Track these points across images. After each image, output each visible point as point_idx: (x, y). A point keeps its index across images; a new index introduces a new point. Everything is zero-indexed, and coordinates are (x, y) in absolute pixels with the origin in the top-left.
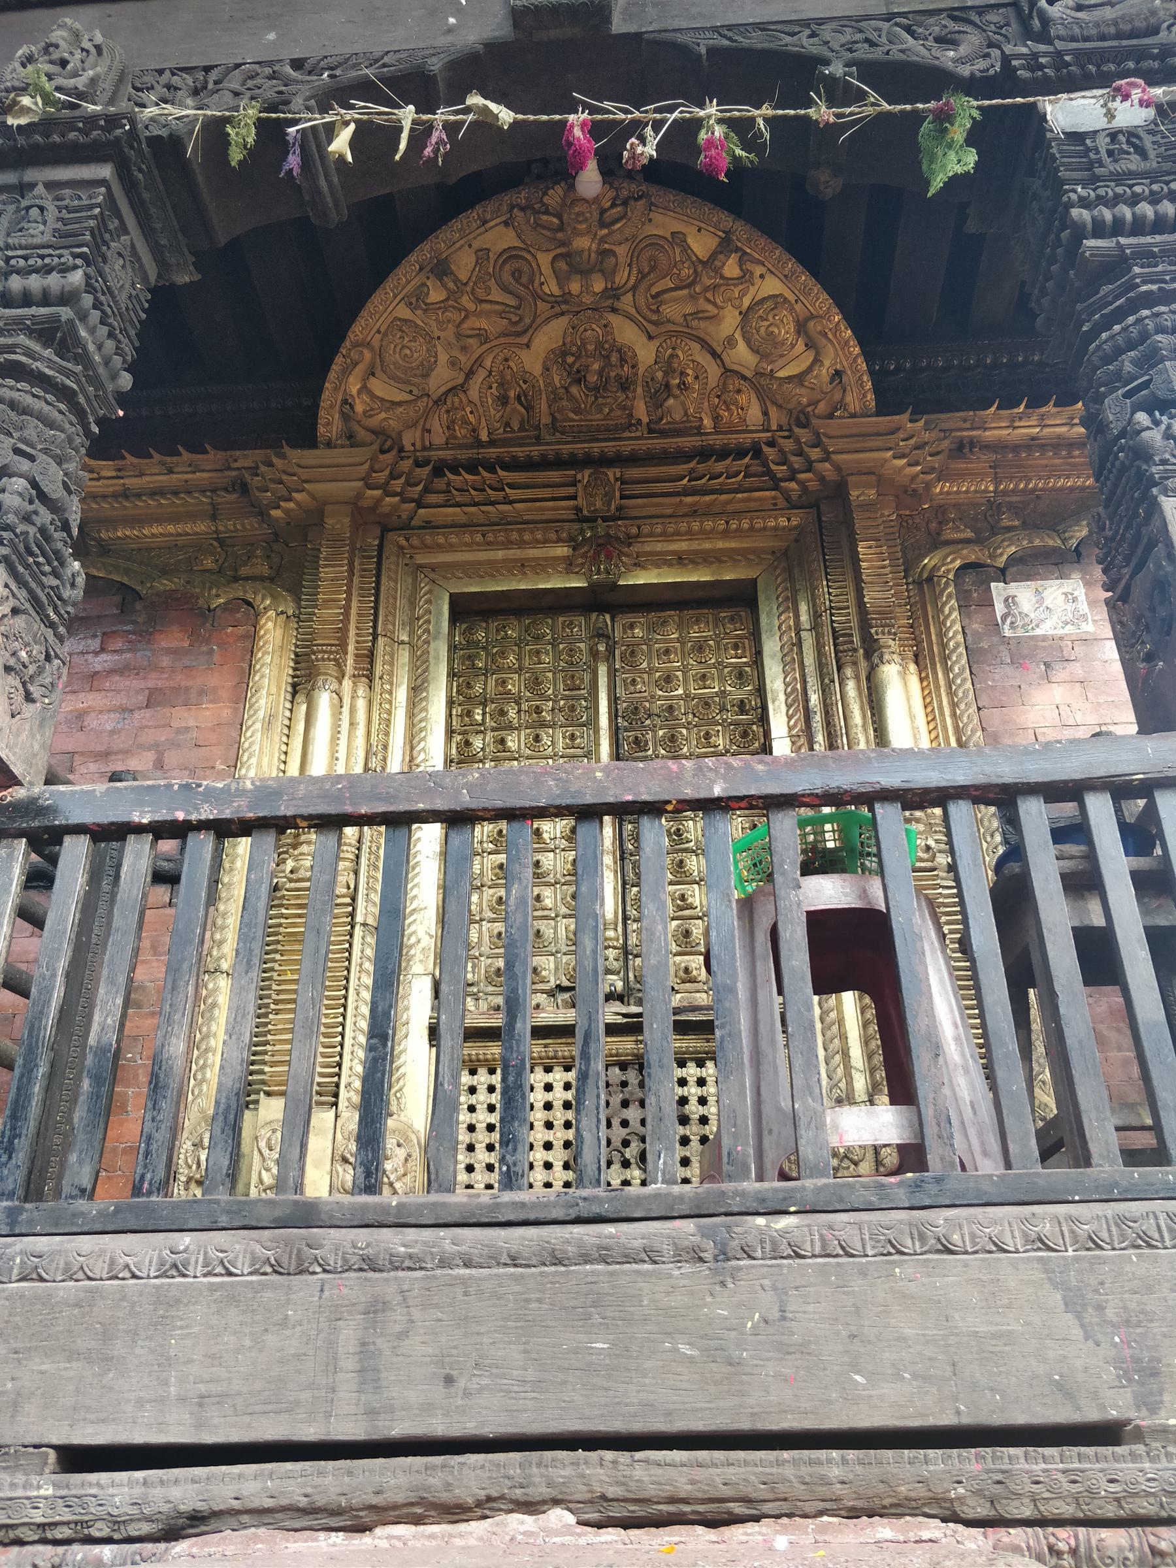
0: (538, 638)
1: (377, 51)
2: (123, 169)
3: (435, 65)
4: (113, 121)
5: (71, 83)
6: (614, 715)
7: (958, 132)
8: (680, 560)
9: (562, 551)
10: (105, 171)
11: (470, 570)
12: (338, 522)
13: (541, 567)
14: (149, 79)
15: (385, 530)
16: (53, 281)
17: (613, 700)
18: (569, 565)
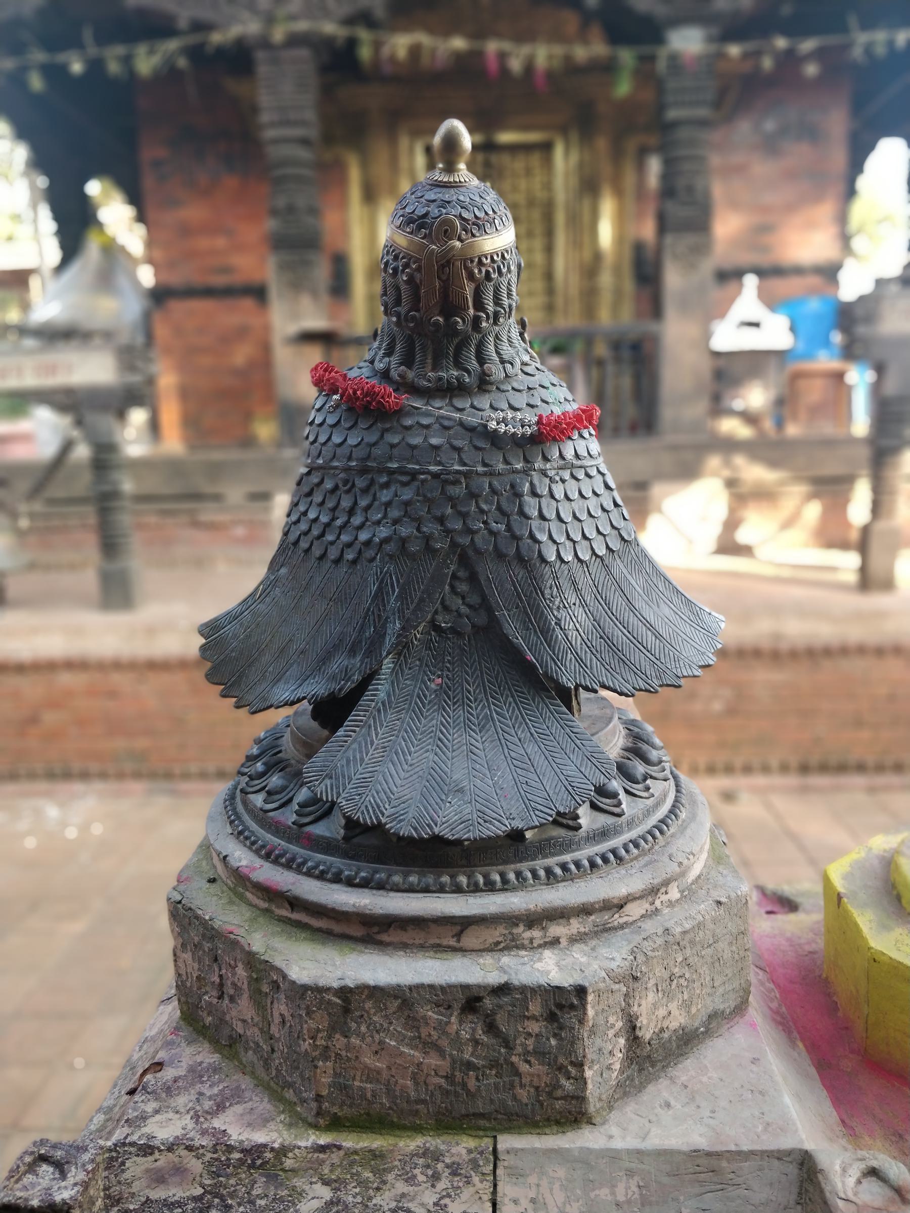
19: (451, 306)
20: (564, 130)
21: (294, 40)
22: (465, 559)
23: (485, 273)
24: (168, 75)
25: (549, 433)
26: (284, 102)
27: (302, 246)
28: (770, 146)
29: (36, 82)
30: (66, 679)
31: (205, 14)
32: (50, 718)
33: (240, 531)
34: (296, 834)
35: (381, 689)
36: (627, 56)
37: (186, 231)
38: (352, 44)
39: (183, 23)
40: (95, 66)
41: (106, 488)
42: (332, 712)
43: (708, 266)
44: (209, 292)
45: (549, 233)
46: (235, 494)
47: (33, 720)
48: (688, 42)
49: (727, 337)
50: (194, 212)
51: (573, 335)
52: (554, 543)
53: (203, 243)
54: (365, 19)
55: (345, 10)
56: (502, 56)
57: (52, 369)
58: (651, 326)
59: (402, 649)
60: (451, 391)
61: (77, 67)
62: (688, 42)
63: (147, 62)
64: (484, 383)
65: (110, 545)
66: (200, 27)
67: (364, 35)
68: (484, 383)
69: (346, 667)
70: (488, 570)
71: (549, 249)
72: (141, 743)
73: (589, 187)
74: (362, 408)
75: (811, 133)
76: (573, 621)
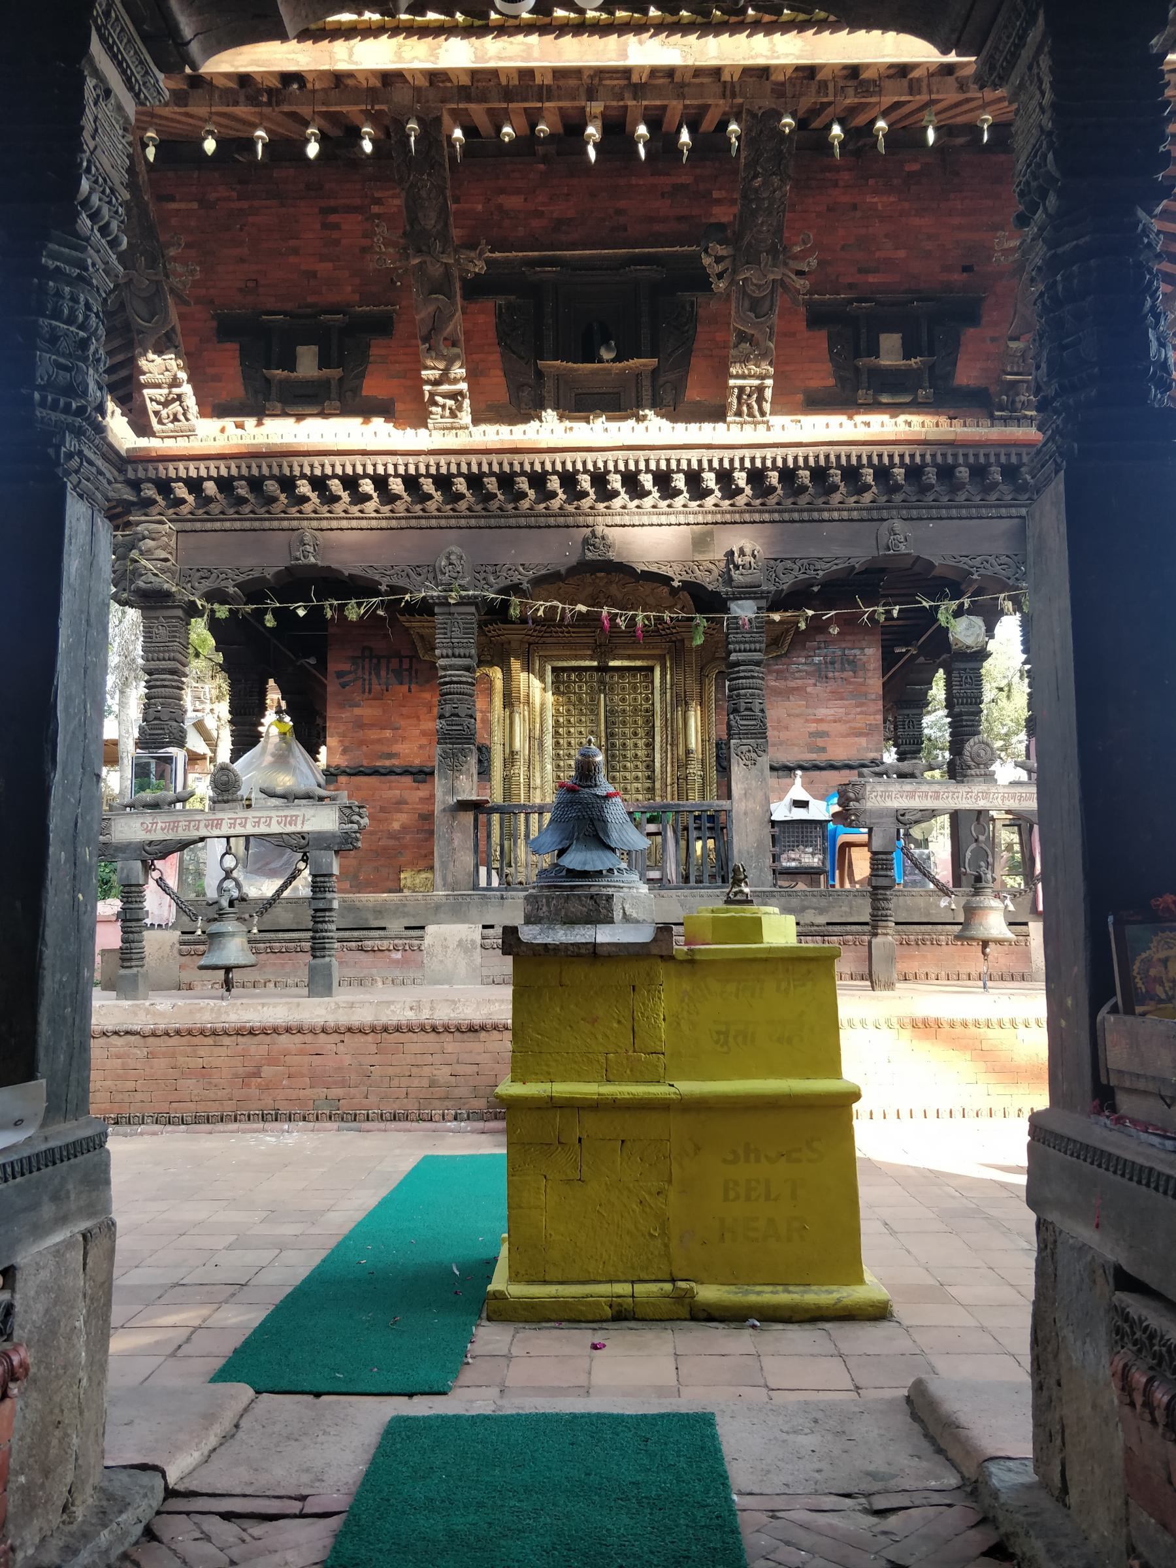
0: (581, 681)
1: (546, 562)
2: (477, 608)
3: (563, 571)
4: (476, 597)
5: (462, 582)
6: (606, 711)
7: (701, 629)
8: (629, 658)
9: (589, 652)
10: (473, 609)
11: (559, 658)
12: (514, 645)
13: (583, 658)
14: (478, 569)
15: (530, 644)
16: (467, 652)
17: (606, 705)
18: (592, 659)
19: (590, 771)
20: (661, 659)
21: (463, 602)
22: (591, 820)
23: (596, 765)
24: (370, 622)
25: (608, 796)
26: (452, 641)
27: (461, 740)
28: (821, 674)
29: (270, 621)
30: (284, 1039)
31: (401, 583)
32: (267, 1071)
33: (398, 955)
34: (556, 877)
35: (573, 847)
36: (700, 620)
37: (360, 725)
38: (505, 604)
39: (383, 588)
40: (316, 613)
41: (321, 905)
42: (562, 852)
43: (764, 761)
44: (376, 772)
45: (651, 734)
46: (395, 926)
47: (257, 1074)
48: (744, 610)
49: (782, 811)
50: (367, 711)
51: (665, 809)
52: (609, 817)
53: (374, 734)
54: (515, 589)
55: (503, 583)
57: (293, 820)
58: (724, 804)
59: (578, 839)
60: (589, 787)
61: (301, 613)
62: (744, 610)
63: (353, 612)
64: (596, 785)
65: (318, 948)
66: (393, 589)
67: (515, 600)
68: (596, 785)
69: (566, 843)
70: (596, 823)
71: (650, 745)
72: (337, 1092)
73: (681, 701)
74: (571, 790)
75: (853, 664)
76: (614, 835)
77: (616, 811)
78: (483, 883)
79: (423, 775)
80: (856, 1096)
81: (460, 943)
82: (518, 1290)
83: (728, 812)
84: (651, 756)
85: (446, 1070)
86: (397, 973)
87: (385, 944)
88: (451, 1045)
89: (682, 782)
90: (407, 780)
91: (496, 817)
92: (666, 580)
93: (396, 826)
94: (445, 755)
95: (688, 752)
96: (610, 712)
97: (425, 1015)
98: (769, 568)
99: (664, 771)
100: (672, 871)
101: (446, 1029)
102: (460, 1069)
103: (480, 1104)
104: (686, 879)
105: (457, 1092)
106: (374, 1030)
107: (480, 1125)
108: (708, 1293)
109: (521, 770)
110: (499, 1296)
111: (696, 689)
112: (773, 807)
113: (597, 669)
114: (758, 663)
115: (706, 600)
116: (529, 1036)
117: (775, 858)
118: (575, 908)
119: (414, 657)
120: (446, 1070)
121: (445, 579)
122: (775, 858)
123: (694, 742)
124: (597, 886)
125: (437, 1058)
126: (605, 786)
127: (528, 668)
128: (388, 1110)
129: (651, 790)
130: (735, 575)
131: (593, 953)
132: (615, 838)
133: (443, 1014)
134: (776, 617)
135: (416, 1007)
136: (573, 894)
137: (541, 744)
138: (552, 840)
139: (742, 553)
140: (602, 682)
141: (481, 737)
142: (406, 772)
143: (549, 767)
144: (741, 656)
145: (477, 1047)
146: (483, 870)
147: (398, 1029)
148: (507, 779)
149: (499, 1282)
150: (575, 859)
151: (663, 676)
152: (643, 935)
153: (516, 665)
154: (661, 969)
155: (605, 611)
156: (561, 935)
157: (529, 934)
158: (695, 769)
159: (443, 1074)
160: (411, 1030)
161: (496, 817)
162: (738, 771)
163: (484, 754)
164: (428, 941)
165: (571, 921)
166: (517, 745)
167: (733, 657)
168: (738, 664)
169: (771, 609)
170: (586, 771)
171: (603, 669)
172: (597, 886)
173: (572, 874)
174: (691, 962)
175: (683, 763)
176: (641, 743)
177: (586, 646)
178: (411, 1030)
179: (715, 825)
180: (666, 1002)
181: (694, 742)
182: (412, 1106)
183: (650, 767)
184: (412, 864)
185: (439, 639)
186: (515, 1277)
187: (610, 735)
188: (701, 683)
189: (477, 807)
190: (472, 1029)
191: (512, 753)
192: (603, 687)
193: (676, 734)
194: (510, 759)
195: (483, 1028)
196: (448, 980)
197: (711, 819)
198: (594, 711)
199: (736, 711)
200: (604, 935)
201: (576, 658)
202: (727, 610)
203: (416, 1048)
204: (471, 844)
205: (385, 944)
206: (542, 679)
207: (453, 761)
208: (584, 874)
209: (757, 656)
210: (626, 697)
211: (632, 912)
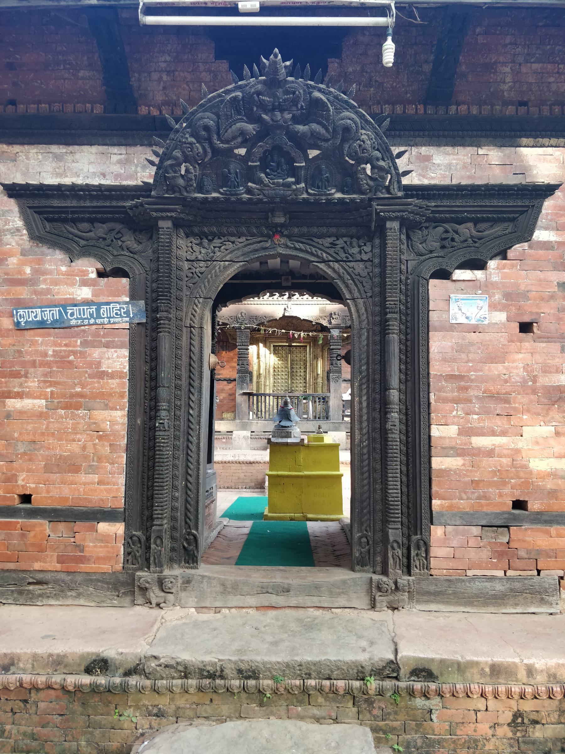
8: (299, 342)
11: (275, 342)
20: (310, 343)
21: (246, 328)
27: (245, 372)
31: (226, 322)
33: (224, 440)
38: (259, 330)
45: (305, 368)
48: (335, 333)
51: (309, 395)
54: (262, 324)
56: (293, 334)
58: (328, 394)
66: (224, 324)
67: (262, 328)
71: (305, 372)
73: (316, 358)
77: (293, 412)
78: (251, 418)
79: (230, 381)
80: (342, 475)
81: (244, 437)
82: (270, 515)
83: (328, 397)
84: (305, 375)
85: (243, 474)
86: (224, 446)
87: (220, 437)
88: (244, 467)
89: (316, 384)
90: (225, 382)
91: (255, 398)
92: (312, 322)
93: (221, 398)
94: (239, 377)
95: (318, 375)
96: (292, 360)
97: (236, 459)
98: (343, 319)
99: (309, 380)
100: (311, 416)
101: (243, 463)
102: (247, 474)
103: (253, 484)
104: (315, 417)
105: (246, 481)
106: (222, 462)
107: (253, 490)
108: (310, 516)
109: (262, 379)
110: (266, 515)
111: (321, 354)
112: (343, 395)
113: (288, 346)
114: (339, 349)
115: (324, 329)
116: (272, 464)
117: (343, 412)
118: (283, 434)
119: (227, 341)
120: (243, 474)
121: (240, 321)
122: (343, 412)
123: (320, 371)
124: (288, 430)
125: (240, 471)
126: (290, 407)
127: (265, 346)
128: (226, 486)
129: (305, 387)
130: (333, 321)
131: (287, 444)
132: (292, 419)
133: (242, 458)
134: (345, 335)
135: (234, 456)
136: (282, 431)
137: (269, 371)
138: (277, 418)
139: (335, 314)
140: (290, 351)
141: (250, 369)
142: (225, 380)
143: (272, 379)
144: (334, 347)
145: (252, 468)
146: (251, 413)
147: (229, 462)
148: (258, 383)
149: (266, 513)
150: (283, 423)
151: (310, 349)
152: (297, 440)
153: (261, 345)
154: (302, 448)
155: (291, 332)
156: (280, 440)
157: (273, 440)
158: (320, 380)
159: (242, 475)
160: (232, 463)
161: (255, 398)
162: (332, 384)
163: (251, 373)
164: (234, 436)
165: (282, 437)
166: (261, 372)
167: (332, 347)
168: (333, 349)
169: (343, 333)
170: (286, 403)
171: (290, 346)
172: (288, 430)
173: (283, 427)
174: (308, 446)
175: (316, 378)
176: (302, 371)
177: (285, 338)
178: (232, 463)
179: (325, 400)
180: (302, 455)
181: (320, 371)
182: (233, 485)
183: (305, 379)
184: (227, 411)
185: (238, 340)
186: (269, 512)
187: (292, 368)
188: (322, 352)
189: (250, 394)
190: (250, 463)
191: (260, 374)
192: (291, 352)
193: (314, 369)
194: (259, 375)
195: (254, 462)
196: (240, 448)
197: (324, 399)
198: (287, 360)
199: (332, 364)
200: (289, 440)
201: (281, 342)
202: (330, 332)
203: (234, 468)
204: (247, 405)
205: (220, 437)
206: (270, 350)
207: (242, 380)
208: (285, 427)
209: (339, 347)
210: (298, 355)
211: (296, 435)
